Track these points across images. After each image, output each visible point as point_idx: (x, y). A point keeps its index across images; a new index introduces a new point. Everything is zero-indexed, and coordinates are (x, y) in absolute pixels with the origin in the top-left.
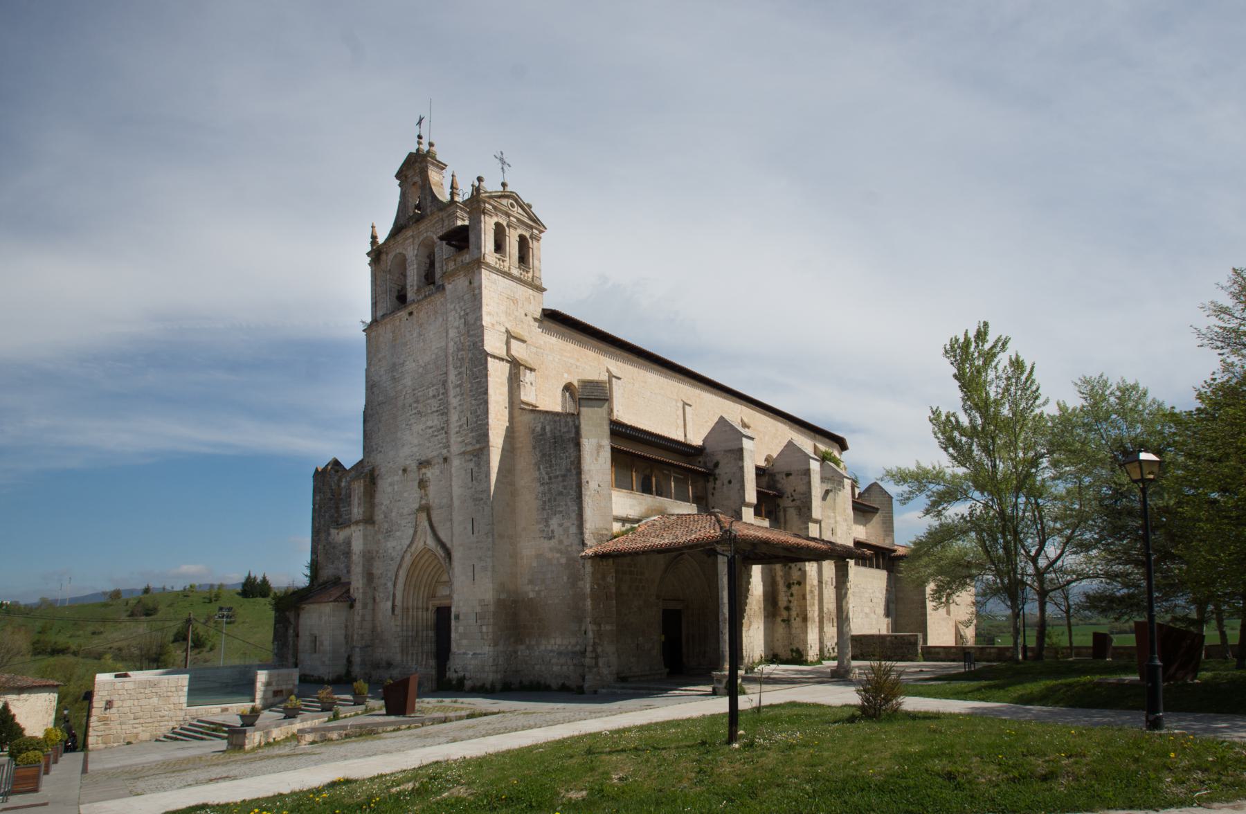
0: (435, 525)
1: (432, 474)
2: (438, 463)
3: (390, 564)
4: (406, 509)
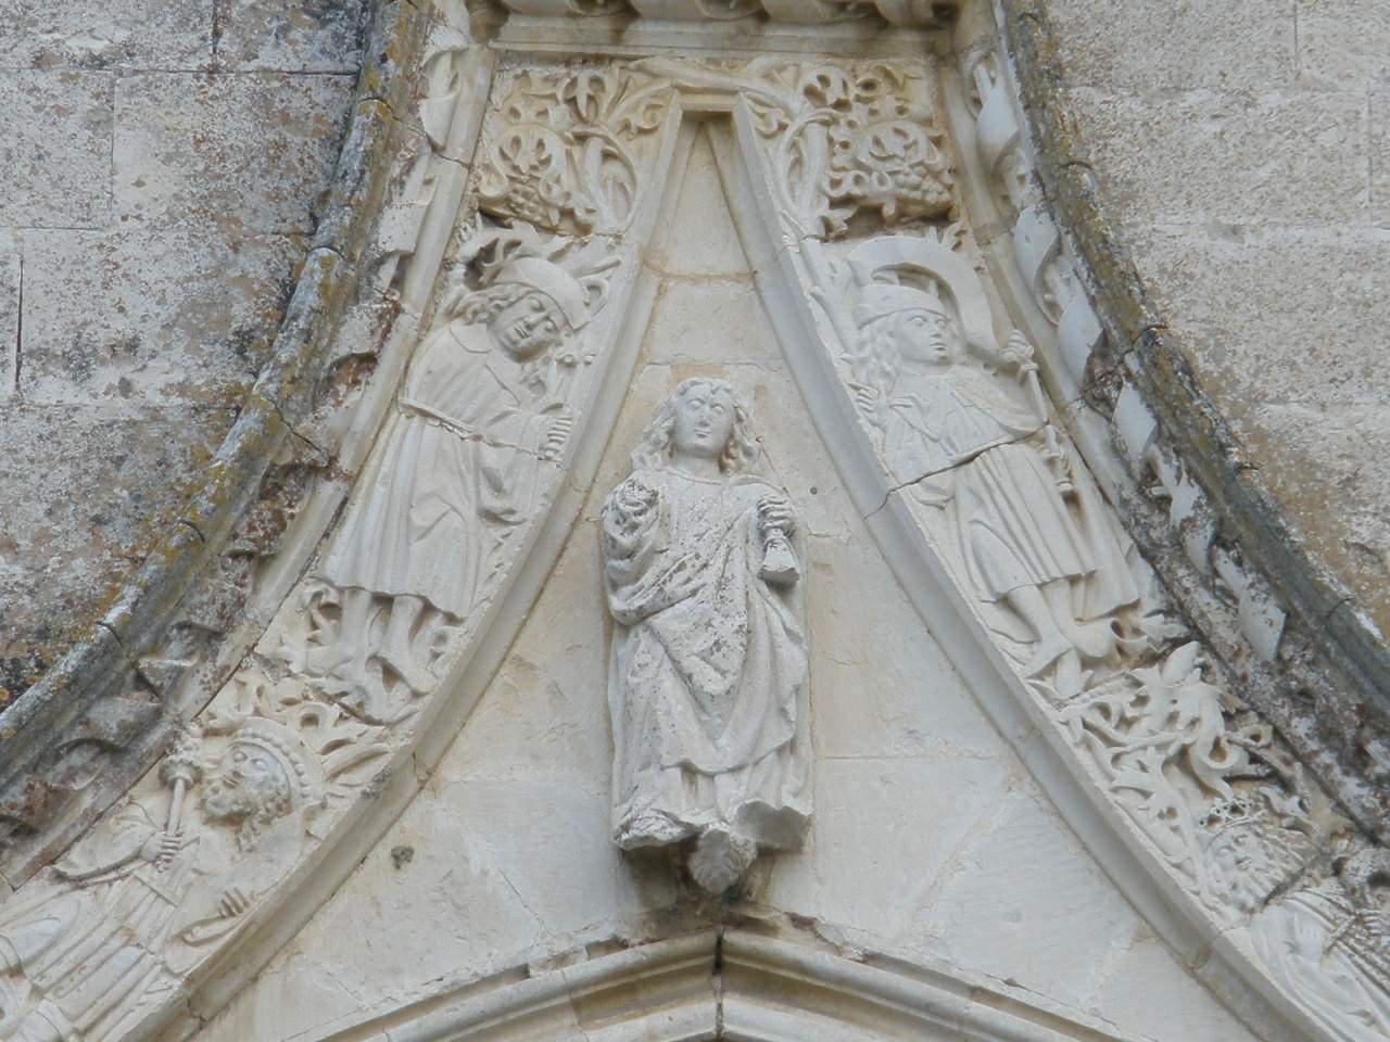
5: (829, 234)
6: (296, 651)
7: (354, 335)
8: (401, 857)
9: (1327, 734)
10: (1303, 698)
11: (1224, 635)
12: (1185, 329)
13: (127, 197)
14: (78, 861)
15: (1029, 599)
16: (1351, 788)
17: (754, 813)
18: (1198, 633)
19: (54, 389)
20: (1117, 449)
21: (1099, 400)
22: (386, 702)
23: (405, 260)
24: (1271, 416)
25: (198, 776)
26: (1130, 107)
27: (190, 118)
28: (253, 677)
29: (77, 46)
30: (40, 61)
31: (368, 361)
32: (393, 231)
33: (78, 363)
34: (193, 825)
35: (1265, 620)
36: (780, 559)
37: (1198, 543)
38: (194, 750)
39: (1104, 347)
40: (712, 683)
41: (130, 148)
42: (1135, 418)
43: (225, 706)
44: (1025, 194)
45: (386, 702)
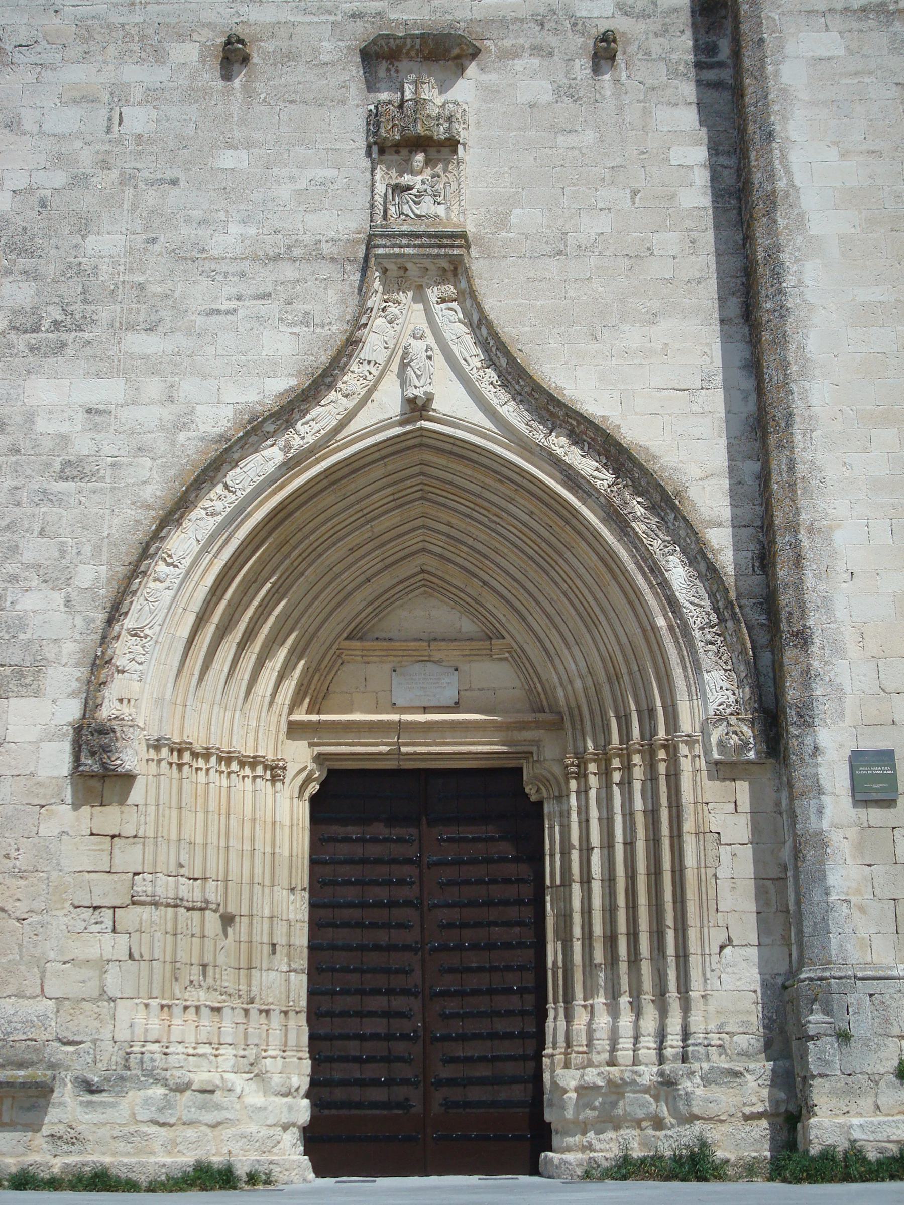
0: (507, 330)
1: (490, 93)
2: (537, 50)
3: (45, 495)
4: (234, 229)
5: (438, 303)
6: (356, 370)
7: (363, 320)
8: (372, 401)
9: (513, 378)
10: (510, 373)
11: (498, 364)
12: (492, 317)
13: (330, 300)
14: (323, 403)
15: (468, 359)
16: (517, 387)
17: (425, 393)
18: (494, 364)
19: (319, 330)
20: (482, 335)
21: (479, 328)
22: (370, 377)
23: (372, 309)
24: (506, 330)
25: (341, 390)
26: (484, 282)
27: (340, 287)
28: (349, 374)
29: (322, 277)
30: (316, 279)
31: (367, 324)
32: (369, 304)
33: (323, 327)
34: (340, 396)
35: (503, 362)
36: (430, 353)
37: (494, 349)
38: (340, 385)
39: (480, 320)
40: (419, 373)
41: (330, 292)
42: (484, 331)
43: (345, 378)
44: (467, 296)
45: (370, 377)
